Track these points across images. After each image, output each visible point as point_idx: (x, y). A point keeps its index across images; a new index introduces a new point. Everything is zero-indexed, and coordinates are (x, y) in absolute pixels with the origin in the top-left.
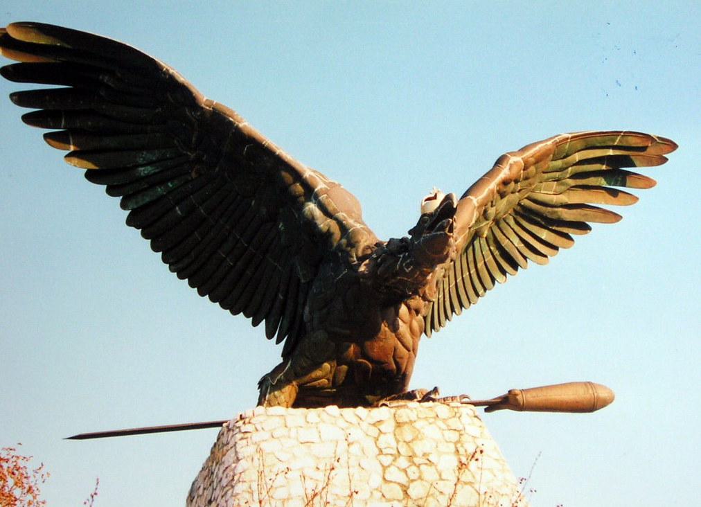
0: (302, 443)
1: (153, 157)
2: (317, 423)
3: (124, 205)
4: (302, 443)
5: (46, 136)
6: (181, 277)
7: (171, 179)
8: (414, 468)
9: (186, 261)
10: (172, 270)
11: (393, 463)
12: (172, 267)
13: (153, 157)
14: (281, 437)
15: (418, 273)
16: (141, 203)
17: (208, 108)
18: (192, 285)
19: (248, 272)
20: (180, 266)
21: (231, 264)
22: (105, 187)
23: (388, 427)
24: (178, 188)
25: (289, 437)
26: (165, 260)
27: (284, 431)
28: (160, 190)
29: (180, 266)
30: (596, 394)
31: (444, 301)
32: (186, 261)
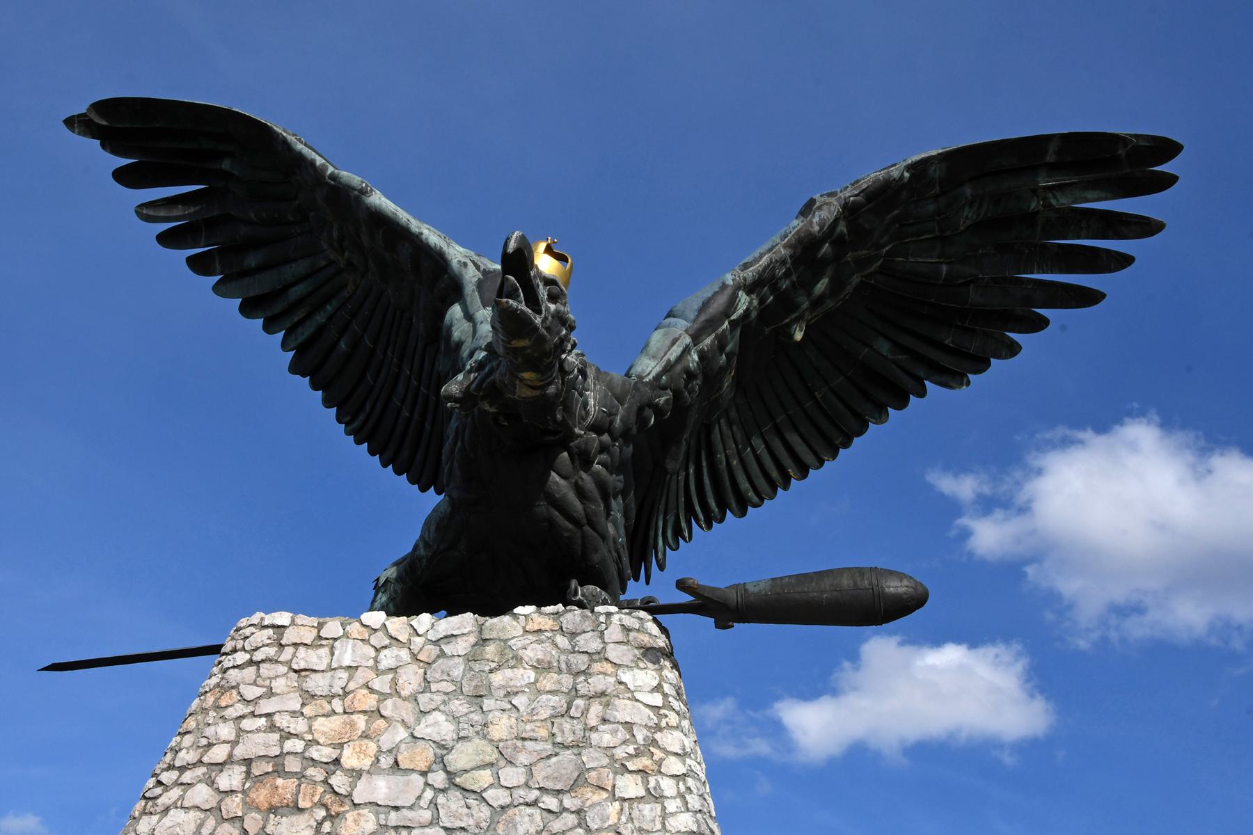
0: (295, 671)
1: (301, 267)
2: (335, 639)
3: (285, 346)
4: (295, 671)
5: (193, 263)
6: (358, 442)
7: (327, 300)
8: (476, 717)
9: (362, 417)
11: (442, 707)
12: (349, 428)
13: (301, 267)
14: (263, 661)
15: (518, 382)
16: (301, 339)
17: (333, 183)
19: (428, 426)
20: (356, 424)
22: (260, 322)
23: (461, 647)
24: (338, 309)
25: (277, 662)
27: (271, 651)
28: (320, 318)
29: (356, 424)
30: (875, 588)
31: (758, 459)
32: (362, 417)
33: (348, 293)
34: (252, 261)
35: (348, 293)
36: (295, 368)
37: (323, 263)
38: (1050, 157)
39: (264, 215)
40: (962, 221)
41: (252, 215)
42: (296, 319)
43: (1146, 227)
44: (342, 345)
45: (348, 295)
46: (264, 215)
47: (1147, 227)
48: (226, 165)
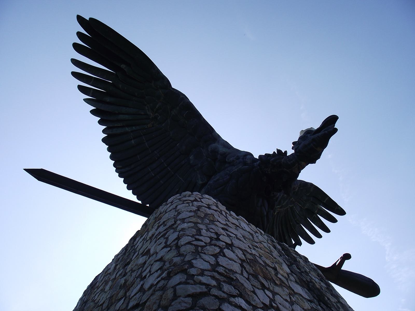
3: (104, 131)
10: (116, 171)
18: (125, 182)
21: (153, 175)
26: (114, 165)
28: (128, 129)
29: (123, 170)
33: (147, 127)
34: (108, 99)
35: (147, 127)
36: (104, 140)
37: (143, 113)
38: (325, 202)
39: (126, 88)
40: (306, 206)
41: (120, 86)
42: (116, 125)
43: (327, 230)
44: (133, 142)
45: (146, 127)
46: (126, 88)
47: (327, 230)
48: (123, 66)
